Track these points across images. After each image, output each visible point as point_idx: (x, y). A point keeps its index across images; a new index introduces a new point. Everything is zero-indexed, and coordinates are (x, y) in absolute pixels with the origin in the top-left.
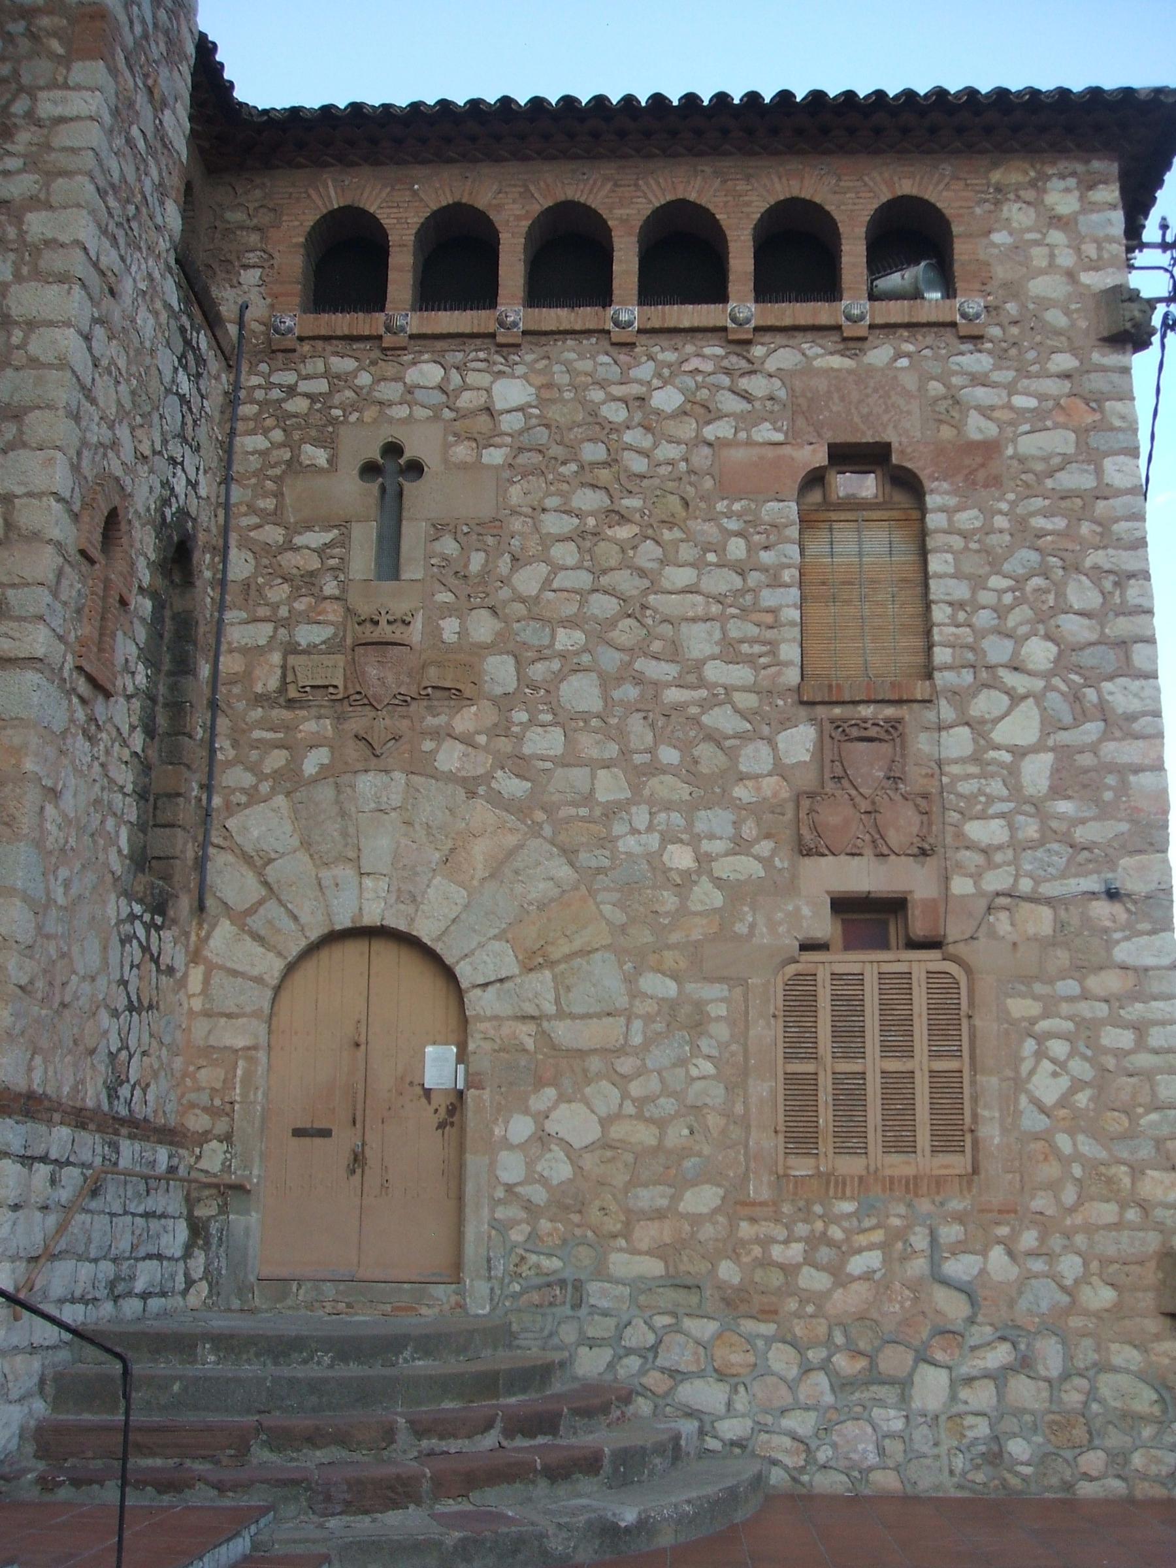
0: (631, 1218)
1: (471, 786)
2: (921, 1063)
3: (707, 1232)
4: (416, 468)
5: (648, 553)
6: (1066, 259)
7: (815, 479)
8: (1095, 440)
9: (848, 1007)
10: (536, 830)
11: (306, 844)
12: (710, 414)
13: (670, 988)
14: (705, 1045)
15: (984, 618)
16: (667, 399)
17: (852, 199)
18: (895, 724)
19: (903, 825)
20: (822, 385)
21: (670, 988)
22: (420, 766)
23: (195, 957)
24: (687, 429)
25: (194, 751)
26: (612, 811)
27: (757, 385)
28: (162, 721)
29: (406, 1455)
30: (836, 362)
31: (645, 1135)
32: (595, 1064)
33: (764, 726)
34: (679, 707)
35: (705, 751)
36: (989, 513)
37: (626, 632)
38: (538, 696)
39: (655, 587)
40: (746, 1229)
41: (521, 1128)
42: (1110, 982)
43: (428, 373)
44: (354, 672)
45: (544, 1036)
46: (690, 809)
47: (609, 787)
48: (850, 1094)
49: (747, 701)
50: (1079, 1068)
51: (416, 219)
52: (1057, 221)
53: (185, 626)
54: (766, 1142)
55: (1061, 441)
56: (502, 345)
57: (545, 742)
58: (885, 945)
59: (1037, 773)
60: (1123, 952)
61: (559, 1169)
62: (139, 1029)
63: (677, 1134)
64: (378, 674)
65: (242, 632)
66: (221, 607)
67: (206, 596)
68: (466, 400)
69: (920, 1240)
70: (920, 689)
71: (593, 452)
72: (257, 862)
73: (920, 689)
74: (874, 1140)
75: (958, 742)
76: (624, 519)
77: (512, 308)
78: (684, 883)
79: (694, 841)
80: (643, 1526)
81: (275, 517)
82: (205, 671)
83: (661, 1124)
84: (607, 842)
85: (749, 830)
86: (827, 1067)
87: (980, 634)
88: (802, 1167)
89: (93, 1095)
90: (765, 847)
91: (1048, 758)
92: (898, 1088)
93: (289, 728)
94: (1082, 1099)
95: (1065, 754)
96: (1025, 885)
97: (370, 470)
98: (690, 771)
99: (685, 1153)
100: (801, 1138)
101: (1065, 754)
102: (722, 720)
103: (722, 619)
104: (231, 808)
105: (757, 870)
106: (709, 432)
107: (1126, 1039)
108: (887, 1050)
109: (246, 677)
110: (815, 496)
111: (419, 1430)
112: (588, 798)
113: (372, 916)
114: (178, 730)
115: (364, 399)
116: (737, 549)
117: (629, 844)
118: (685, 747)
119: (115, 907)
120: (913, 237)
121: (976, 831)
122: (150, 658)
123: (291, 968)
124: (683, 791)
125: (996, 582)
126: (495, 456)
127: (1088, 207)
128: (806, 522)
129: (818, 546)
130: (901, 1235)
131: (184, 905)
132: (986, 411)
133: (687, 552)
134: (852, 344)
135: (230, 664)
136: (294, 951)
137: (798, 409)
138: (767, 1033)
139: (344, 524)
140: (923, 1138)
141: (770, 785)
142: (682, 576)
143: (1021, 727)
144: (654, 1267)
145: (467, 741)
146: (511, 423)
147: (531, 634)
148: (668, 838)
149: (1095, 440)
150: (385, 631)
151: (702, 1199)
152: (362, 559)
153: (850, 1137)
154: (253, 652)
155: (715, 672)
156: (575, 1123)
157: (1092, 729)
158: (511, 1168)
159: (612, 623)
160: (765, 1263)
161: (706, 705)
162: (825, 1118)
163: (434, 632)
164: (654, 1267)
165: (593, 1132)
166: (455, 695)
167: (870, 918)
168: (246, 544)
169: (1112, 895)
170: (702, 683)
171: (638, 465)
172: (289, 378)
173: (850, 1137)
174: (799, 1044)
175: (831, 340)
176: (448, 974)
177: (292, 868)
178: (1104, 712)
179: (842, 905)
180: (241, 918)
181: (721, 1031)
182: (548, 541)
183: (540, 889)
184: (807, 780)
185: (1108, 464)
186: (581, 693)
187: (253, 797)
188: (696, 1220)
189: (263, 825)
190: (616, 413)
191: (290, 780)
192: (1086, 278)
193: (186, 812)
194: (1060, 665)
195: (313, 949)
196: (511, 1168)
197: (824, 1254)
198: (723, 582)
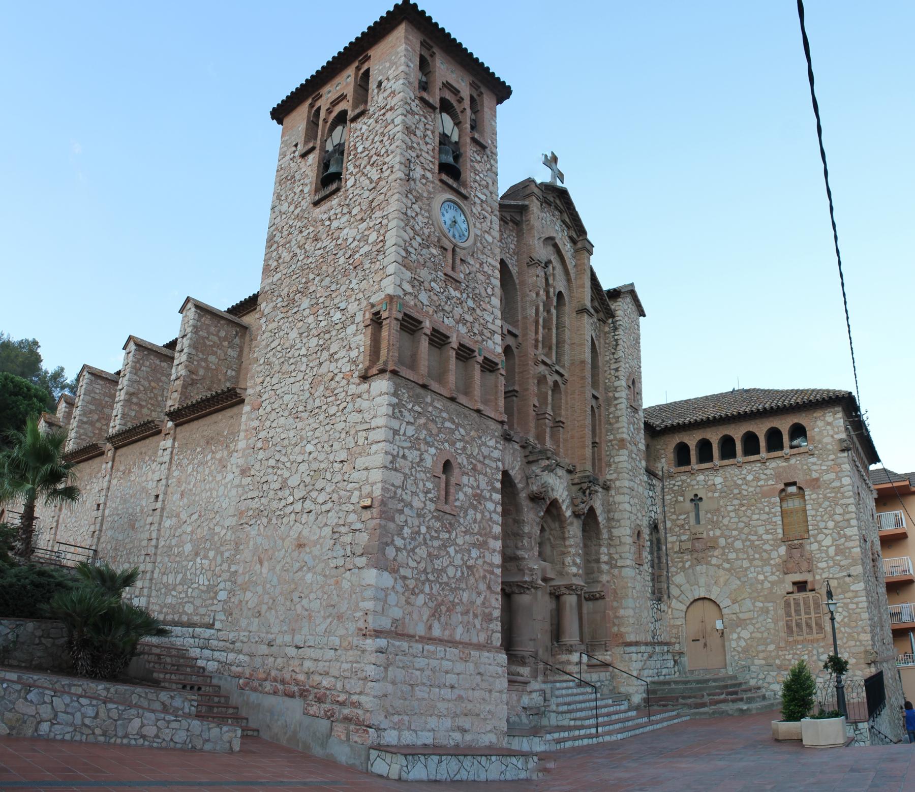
0: (758, 652)
1: (718, 566)
2: (813, 615)
3: (773, 654)
4: (701, 499)
5: (749, 513)
6: (831, 433)
7: (783, 490)
8: (840, 474)
9: (797, 605)
10: (732, 574)
11: (688, 582)
12: (759, 480)
13: (761, 605)
14: (770, 616)
15: (819, 518)
16: (750, 477)
17: (784, 425)
18: (801, 544)
19: (804, 566)
20: (781, 470)
21: (761, 605)
22: (708, 563)
23: (669, 607)
24: (755, 484)
25: (664, 565)
26: (747, 569)
27: (768, 472)
28: (656, 561)
29: (706, 699)
30: (784, 464)
31: (759, 635)
32: (748, 622)
33: (776, 547)
34: (758, 545)
35: (764, 554)
36: (818, 494)
37: (746, 530)
38: (729, 546)
39: (751, 520)
40: (780, 653)
41: (735, 636)
42: (850, 594)
43: (701, 477)
44: (693, 545)
45: (738, 617)
46: (762, 567)
47: (746, 564)
48: (799, 623)
49: (771, 542)
50: (845, 613)
52: (829, 424)
53: (659, 541)
54: (783, 634)
55: (832, 476)
56: (715, 469)
57: (732, 556)
58: (805, 590)
59: (832, 551)
60: (852, 588)
61: (743, 644)
62: (658, 625)
63: (765, 635)
64: (698, 545)
65: (670, 539)
66: (666, 533)
67: (662, 532)
68: (710, 483)
69: (815, 652)
70: (806, 536)
71: (736, 491)
72: (679, 586)
73: (806, 536)
74: (805, 632)
75: (815, 546)
76: (743, 505)
77: (717, 461)
78: (762, 582)
79: (763, 574)
80: (748, 709)
81: (674, 513)
82: (664, 548)
83: (762, 633)
84: (746, 576)
85: (774, 570)
86: (794, 618)
87: (818, 522)
88: (791, 639)
89: (649, 639)
90: (778, 573)
92: (808, 621)
93: (682, 558)
94: (846, 620)
95: (837, 546)
96: (831, 576)
97: (692, 500)
98: (761, 559)
99: (768, 638)
100: (790, 633)
101: (837, 546)
102: (767, 547)
103: (765, 525)
104: (673, 576)
105: (777, 578)
106: (759, 484)
107: (854, 606)
108: (806, 613)
109: (673, 548)
110: (784, 494)
111: (709, 695)
112: (742, 567)
113: (702, 595)
114: (660, 562)
115: (689, 485)
116: (767, 509)
117: (750, 575)
118: (760, 554)
119: (649, 603)
120: (798, 431)
121: (820, 565)
122: (651, 553)
123: (688, 607)
124: (760, 563)
125: (821, 510)
126: (716, 495)
127: (835, 419)
128: (782, 500)
129: (785, 505)
130: (811, 651)
131: (665, 597)
133: (757, 511)
134: (787, 460)
135: (669, 546)
136: (688, 604)
137: (777, 476)
138: (781, 612)
139: (688, 513)
140: (814, 631)
141: (777, 560)
142: (756, 517)
143: (828, 541)
144: (763, 662)
145: (717, 557)
146: (719, 487)
147: (727, 533)
148: (758, 573)
149: (840, 474)
150: (698, 536)
151: (771, 647)
152: (692, 521)
153: (800, 632)
154: (673, 543)
155: (765, 537)
156: (745, 634)
157: (843, 540)
158: (734, 644)
159: (743, 529)
160: (785, 659)
161: (763, 544)
162: (794, 629)
163: (708, 535)
164: (763, 662)
165: (749, 636)
166: (713, 548)
167: (801, 586)
168: (669, 520)
169: (849, 576)
170: (762, 540)
171: (745, 493)
172: (673, 482)
173: (800, 632)
174: (788, 614)
175: (782, 460)
176: (718, 606)
177: (686, 587)
178: (845, 536)
179: (794, 583)
180: (677, 598)
181: (772, 613)
182: (729, 512)
183: (735, 587)
184: (785, 558)
185: (843, 479)
186: (738, 544)
187: (677, 573)
188: (770, 652)
189: (679, 579)
190: (740, 482)
191: (683, 569)
192: (836, 436)
193: (664, 579)
194: (835, 527)
195: (692, 603)
196: (734, 644)
197: (796, 657)
198: (765, 517)
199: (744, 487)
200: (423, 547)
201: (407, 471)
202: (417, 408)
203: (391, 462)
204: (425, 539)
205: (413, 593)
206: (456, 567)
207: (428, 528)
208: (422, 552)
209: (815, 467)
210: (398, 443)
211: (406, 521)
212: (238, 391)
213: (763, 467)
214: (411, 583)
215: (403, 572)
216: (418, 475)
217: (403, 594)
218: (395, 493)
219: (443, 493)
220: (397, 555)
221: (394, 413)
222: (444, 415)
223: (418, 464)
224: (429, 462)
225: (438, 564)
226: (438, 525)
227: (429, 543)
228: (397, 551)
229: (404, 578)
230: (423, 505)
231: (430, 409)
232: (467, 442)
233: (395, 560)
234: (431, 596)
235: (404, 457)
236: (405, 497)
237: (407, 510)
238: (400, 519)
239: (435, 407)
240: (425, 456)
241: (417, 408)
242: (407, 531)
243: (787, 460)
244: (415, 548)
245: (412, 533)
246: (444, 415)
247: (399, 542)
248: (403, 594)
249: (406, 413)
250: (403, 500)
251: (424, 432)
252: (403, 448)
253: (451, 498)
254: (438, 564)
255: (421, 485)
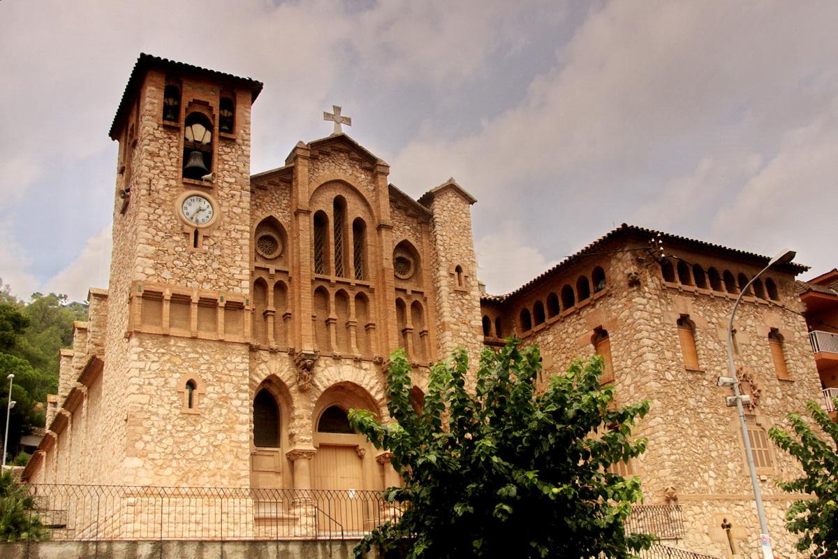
16: (570, 330)
30: (593, 310)
51: (532, 307)
55: (626, 313)
59: (632, 388)
91: (633, 385)
101: (636, 383)
132: (614, 311)
146: (552, 344)
171: (568, 346)
199: (567, 340)
200: (170, 438)
201: (153, 392)
202: (162, 350)
203: (138, 389)
204: (171, 433)
205: (161, 467)
206: (202, 448)
207: (174, 426)
208: (169, 441)
209: (614, 307)
210: (143, 377)
211: (153, 424)
212: (98, 357)
213: (579, 317)
214: (160, 462)
215: (151, 456)
216: (163, 394)
217: (152, 469)
218: (142, 408)
219: (188, 401)
220: (145, 446)
221: (139, 358)
222: (188, 350)
223: (163, 386)
224: (173, 383)
225: (183, 447)
226: (183, 422)
227: (175, 435)
228: (145, 444)
229: (153, 459)
230: (168, 412)
231: (173, 349)
232: (212, 363)
233: (143, 449)
234: (179, 468)
235: (150, 384)
236: (150, 408)
237: (153, 418)
238: (147, 424)
239: (179, 346)
240: (170, 380)
241: (162, 350)
242: (153, 430)
243: (594, 306)
244: (162, 439)
245: (159, 431)
246: (188, 350)
247: (147, 438)
248: (152, 469)
249: (151, 356)
250: (149, 411)
251: (169, 365)
252: (149, 378)
253: (195, 403)
254: (183, 447)
255: (166, 400)
